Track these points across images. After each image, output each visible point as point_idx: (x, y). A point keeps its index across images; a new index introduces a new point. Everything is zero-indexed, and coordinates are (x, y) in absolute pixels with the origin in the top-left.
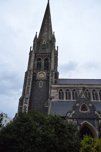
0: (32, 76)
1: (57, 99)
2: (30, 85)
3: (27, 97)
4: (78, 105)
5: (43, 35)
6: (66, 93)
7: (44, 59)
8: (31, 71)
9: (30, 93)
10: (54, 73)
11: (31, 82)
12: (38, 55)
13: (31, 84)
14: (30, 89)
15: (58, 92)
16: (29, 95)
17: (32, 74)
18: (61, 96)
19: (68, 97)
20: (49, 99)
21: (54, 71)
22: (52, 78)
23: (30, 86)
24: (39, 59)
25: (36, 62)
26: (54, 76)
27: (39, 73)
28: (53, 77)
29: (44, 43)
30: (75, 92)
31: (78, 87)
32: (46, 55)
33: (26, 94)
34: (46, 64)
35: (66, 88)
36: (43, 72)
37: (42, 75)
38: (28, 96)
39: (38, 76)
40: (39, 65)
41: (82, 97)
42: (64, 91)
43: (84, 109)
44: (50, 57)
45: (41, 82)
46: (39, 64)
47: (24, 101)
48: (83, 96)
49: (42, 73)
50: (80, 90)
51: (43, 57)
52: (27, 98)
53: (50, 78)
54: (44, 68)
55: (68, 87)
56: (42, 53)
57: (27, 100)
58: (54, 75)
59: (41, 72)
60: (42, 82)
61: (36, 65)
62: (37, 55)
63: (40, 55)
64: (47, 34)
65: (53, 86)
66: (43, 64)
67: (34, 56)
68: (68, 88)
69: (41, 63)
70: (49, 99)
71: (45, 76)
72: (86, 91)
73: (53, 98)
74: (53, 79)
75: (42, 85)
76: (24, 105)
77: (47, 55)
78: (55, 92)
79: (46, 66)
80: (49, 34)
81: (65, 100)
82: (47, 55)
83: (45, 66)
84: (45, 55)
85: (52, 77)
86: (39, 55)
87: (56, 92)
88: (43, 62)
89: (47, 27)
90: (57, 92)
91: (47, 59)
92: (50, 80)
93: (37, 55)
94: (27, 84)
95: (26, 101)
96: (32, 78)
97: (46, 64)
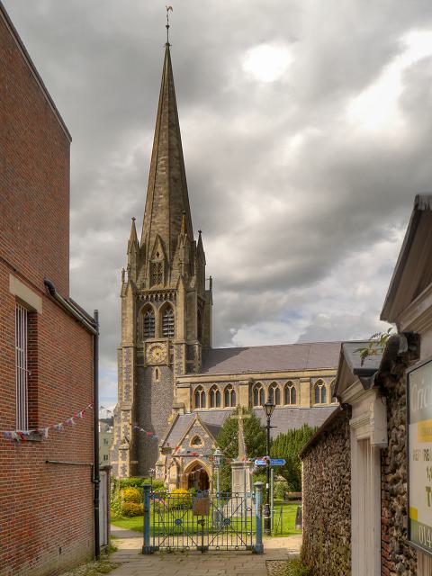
9: (132, 397)
10: (183, 347)
11: (132, 374)
13: (132, 378)
14: (132, 389)
23: (132, 384)
24: (149, 308)
25: (141, 317)
26: (183, 356)
27: (150, 347)
35: (211, 382)
36: (159, 344)
38: (130, 405)
42: (206, 389)
47: (123, 417)
49: (153, 348)
52: (128, 411)
60: (159, 372)
62: (141, 296)
65: (181, 380)
75: (159, 376)
87: (189, 394)
92: (175, 367)
93: (141, 296)
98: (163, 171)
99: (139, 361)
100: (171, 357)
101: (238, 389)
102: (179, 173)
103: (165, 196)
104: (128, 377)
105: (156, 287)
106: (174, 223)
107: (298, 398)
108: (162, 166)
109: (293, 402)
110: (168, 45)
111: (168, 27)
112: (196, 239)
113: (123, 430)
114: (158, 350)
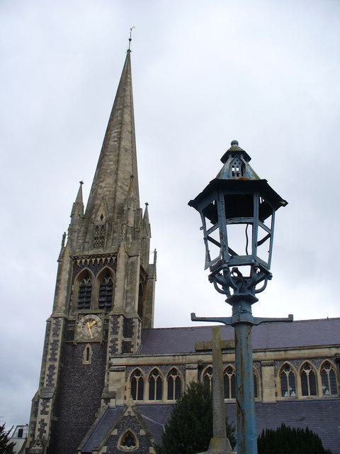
0: (60, 333)
1: (125, 398)
2: (55, 360)
3: (47, 397)
4: (115, 432)
6: (151, 381)
7: (97, 276)
8: (60, 319)
9: (55, 382)
10: (121, 320)
11: (58, 352)
12: (81, 262)
13: (58, 357)
15: (129, 378)
16: (53, 390)
17: (61, 327)
18: (137, 391)
19: (156, 392)
20: (103, 400)
21: (119, 316)
22: (114, 336)
23: (57, 364)
24: (86, 275)
25: (76, 287)
26: (120, 331)
27: (83, 320)
28: (117, 333)
29: (102, 217)
30: (174, 377)
31: (184, 361)
32: (104, 259)
33: (45, 385)
34: (105, 291)
35: (152, 365)
37: (89, 329)
39: (79, 330)
40: (85, 293)
41: (126, 414)
42: (146, 376)
43: (129, 441)
44: (115, 266)
45: (88, 349)
46: (86, 289)
47: (40, 408)
48: (129, 412)
50: (187, 371)
51: (96, 266)
52: (49, 399)
53: (110, 339)
54: (100, 302)
55: (155, 363)
56: (93, 256)
57: (48, 404)
58: (121, 328)
59: (87, 317)
60: (90, 349)
61: (76, 295)
62: (78, 261)
63: (86, 261)
64: (112, 182)
65: (114, 361)
66: (95, 292)
67: (68, 269)
68: (157, 365)
70: (103, 400)
71: (100, 329)
72: (205, 373)
73: (114, 395)
74: (117, 340)
75: (90, 357)
76: (40, 417)
77: (106, 260)
78: (119, 381)
79: (104, 296)
80: (119, 184)
81: (146, 400)
82: (106, 260)
83: (100, 296)
84: (101, 260)
85: (114, 334)
86: (83, 261)
87: (123, 380)
88: (96, 284)
89: (115, 159)
90: (126, 378)
92: (109, 344)
93: (78, 261)
94: (49, 357)
95: (45, 406)
96: (60, 338)
97: (104, 288)
99: (69, 333)
100: (106, 331)
101: (185, 376)
102: (130, 145)
104: (54, 354)
106: (121, 187)
108: (114, 137)
110: (129, 51)
111: (130, 40)
112: (142, 206)
113: (38, 426)
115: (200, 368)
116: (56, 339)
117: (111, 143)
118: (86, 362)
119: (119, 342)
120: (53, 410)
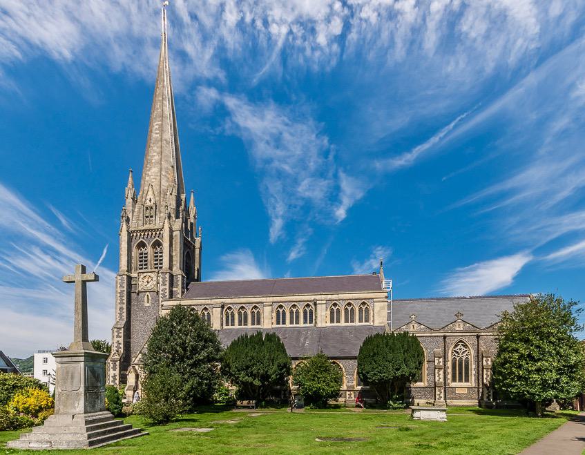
5: (148, 175)
9: (125, 318)
10: (167, 276)
13: (125, 301)
14: (125, 310)
23: (125, 306)
26: (168, 283)
27: (142, 277)
29: (150, 200)
31: (212, 303)
36: (150, 274)
39: (140, 283)
40: (143, 259)
46: (144, 255)
54: (156, 264)
59: (145, 274)
60: (150, 298)
65: (165, 303)
69: (147, 254)
74: (166, 289)
75: (150, 301)
80: (163, 173)
88: (149, 250)
89: (158, 150)
91: (158, 244)
92: (161, 292)
98: (157, 134)
103: (158, 154)
104: (122, 300)
105: (147, 227)
107: (262, 320)
109: (259, 323)
114: (146, 280)
115: (223, 307)
116: (122, 289)
117: (154, 135)
118: (148, 305)
119: (167, 291)
120: (124, 335)
